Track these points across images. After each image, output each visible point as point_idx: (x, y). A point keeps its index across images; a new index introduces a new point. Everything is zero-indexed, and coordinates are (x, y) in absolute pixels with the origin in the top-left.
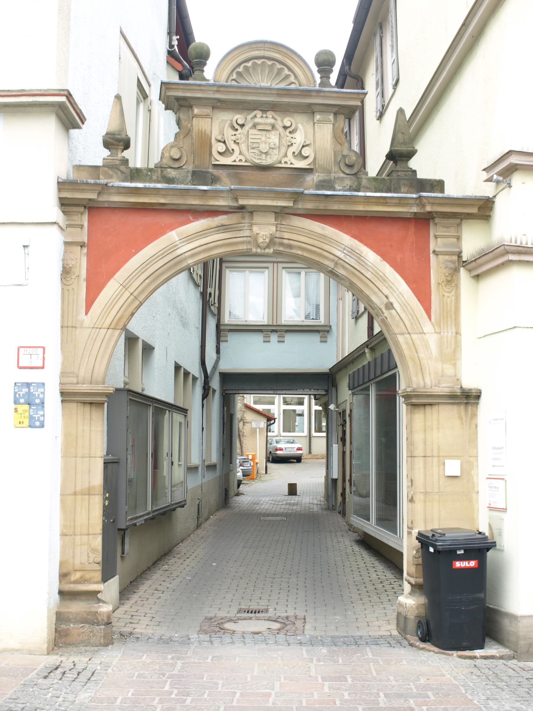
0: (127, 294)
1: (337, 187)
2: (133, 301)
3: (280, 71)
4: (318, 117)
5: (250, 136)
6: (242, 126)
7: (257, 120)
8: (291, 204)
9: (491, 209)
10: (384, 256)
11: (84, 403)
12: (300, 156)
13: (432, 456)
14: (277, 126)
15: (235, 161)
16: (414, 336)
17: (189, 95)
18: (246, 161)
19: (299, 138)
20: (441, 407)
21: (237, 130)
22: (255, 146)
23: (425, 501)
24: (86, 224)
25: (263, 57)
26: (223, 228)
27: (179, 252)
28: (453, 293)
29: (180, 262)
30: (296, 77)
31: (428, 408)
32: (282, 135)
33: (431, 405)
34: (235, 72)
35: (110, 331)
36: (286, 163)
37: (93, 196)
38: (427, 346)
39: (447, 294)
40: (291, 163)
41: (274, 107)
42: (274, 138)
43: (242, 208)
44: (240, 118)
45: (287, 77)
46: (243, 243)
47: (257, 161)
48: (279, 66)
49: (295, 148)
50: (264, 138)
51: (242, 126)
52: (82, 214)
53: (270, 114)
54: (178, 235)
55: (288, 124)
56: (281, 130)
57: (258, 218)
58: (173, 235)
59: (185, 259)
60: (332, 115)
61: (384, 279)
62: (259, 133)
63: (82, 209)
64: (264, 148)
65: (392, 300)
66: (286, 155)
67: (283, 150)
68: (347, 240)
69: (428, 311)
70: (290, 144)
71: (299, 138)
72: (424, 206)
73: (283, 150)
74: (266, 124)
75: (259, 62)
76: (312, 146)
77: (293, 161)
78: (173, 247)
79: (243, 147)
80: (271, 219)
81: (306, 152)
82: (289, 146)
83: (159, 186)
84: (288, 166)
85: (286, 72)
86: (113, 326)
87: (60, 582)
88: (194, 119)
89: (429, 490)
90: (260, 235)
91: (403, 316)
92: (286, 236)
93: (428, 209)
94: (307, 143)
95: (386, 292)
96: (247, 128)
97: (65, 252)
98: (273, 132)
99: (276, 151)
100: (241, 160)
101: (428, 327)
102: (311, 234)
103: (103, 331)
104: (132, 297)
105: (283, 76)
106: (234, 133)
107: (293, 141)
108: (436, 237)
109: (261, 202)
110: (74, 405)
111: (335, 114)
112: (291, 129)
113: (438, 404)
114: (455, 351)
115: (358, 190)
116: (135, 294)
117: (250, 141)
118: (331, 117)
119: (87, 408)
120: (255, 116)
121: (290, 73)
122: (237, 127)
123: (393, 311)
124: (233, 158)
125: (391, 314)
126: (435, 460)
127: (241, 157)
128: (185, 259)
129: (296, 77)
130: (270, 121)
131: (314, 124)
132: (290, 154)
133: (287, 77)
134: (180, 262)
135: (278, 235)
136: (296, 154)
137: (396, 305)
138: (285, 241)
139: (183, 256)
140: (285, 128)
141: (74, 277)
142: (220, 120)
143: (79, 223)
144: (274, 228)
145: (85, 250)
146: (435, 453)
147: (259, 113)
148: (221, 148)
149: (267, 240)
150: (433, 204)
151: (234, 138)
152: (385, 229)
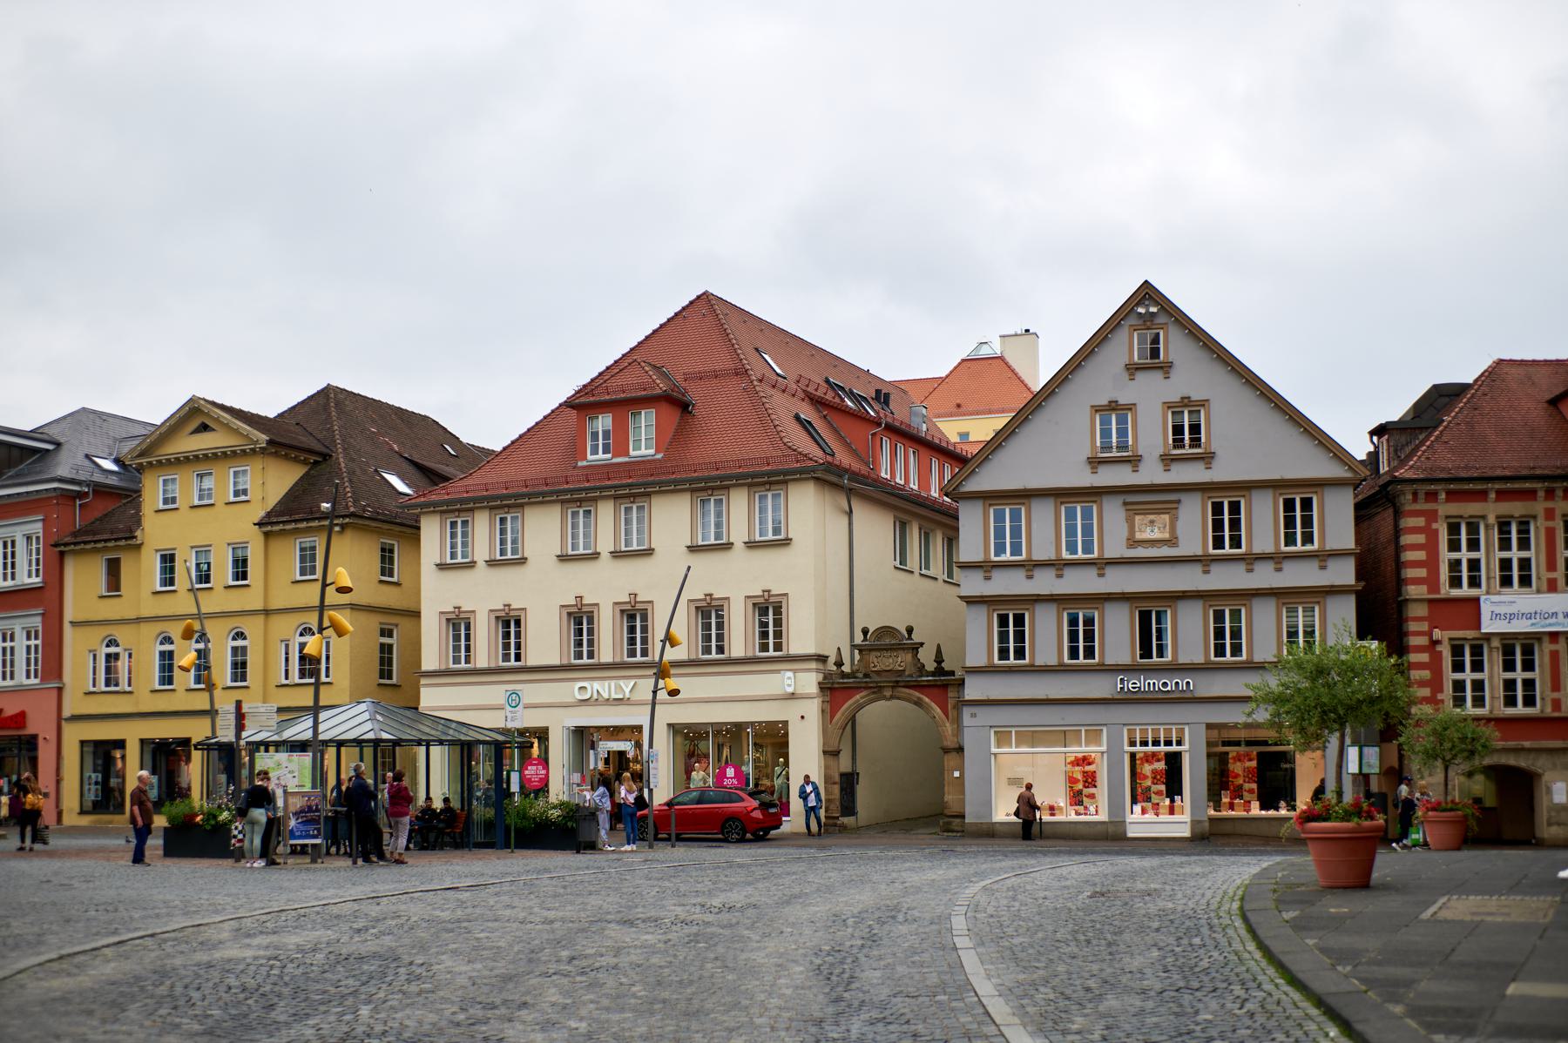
26: (874, 693)
42: (891, 660)
58: (858, 697)
68: (917, 694)
71: (899, 659)
101: (948, 725)
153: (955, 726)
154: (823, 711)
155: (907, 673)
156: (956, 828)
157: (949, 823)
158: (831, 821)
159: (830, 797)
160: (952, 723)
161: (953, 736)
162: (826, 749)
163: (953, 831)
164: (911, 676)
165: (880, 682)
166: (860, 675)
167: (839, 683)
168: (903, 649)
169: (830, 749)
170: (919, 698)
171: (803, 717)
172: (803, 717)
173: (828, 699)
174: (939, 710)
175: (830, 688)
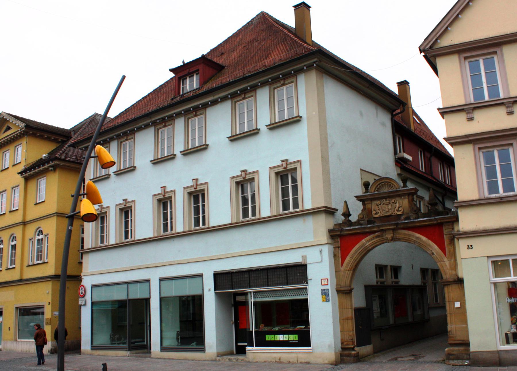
0: (353, 260)
1: (411, 218)
4: (402, 197)
5: (383, 207)
6: (380, 204)
12: (398, 211)
13: (451, 301)
14: (391, 203)
15: (379, 215)
16: (442, 263)
18: (383, 215)
21: (379, 206)
22: (384, 210)
24: (339, 241)
26: (378, 236)
27: (366, 245)
28: (452, 247)
29: (367, 248)
30: (395, 186)
32: (392, 205)
33: (449, 285)
35: (349, 271)
36: (395, 213)
37: (339, 233)
38: (446, 265)
39: (450, 248)
40: (396, 213)
42: (390, 207)
43: (382, 230)
44: (379, 202)
46: (385, 240)
47: (385, 215)
49: (397, 208)
50: (387, 207)
51: (380, 204)
52: (338, 238)
53: (388, 199)
54: (365, 240)
55: (393, 201)
56: (392, 203)
57: (387, 232)
58: (364, 241)
59: (368, 247)
60: (407, 196)
61: (430, 245)
63: (337, 237)
65: (433, 252)
66: (394, 211)
67: (393, 210)
71: (397, 205)
73: (393, 210)
74: (387, 203)
75: (383, 184)
76: (402, 207)
77: (397, 212)
78: (364, 244)
79: (381, 211)
81: (400, 209)
84: (395, 214)
85: (392, 185)
86: (350, 270)
89: (451, 312)
90: (388, 237)
91: (437, 256)
94: (401, 206)
95: (431, 249)
96: (382, 205)
98: (389, 205)
99: (391, 210)
100: (381, 215)
101: (445, 259)
103: (347, 271)
104: (354, 261)
105: (391, 186)
106: (378, 207)
107: (396, 206)
112: (395, 203)
113: (451, 284)
115: (418, 218)
116: (355, 259)
117: (383, 208)
118: (407, 197)
120: (384, 201)
121: (393, 185)
122: (379, 205)
123: (434, 255)
124: (379, 214)
125: (433, 256)
126: (452, 302)
127: (381, 214)
128: (368, 247)
129: (395, 186)
130: (388, 201)
132: (395, 210)
133: (393, 186)
134: (367, 248)
135: (395, 236)
137: (435, 253)
138: (398, 238)
139: (367, 247)
140: (393, 203)
141: (337, 257)
142: (374, 204)
143: (337, 241)
145: (340, 248)
146: (452, 301)
147: (384, 200)
149: (391, 238)
151: (378, 208)
154: (335, 256)
168: (400, 196)
174: (436, 247)
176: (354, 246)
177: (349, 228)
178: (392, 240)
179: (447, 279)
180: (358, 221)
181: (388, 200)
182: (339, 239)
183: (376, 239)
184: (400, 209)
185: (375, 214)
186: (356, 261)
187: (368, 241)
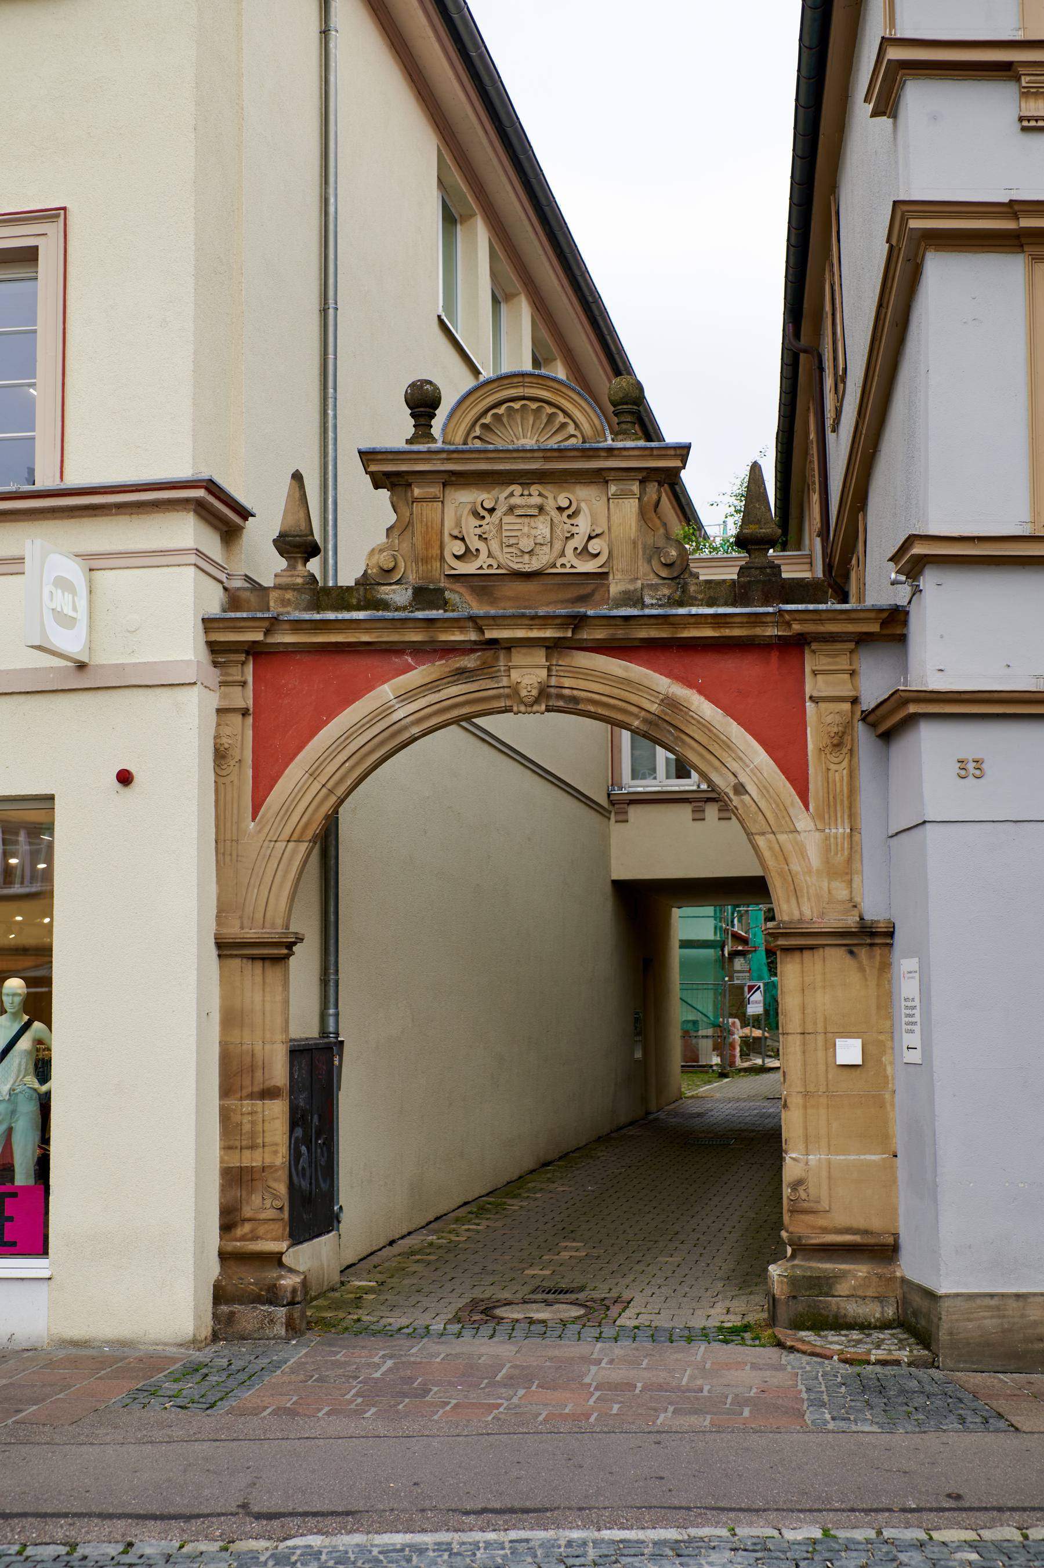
0: (317, 786)
1: (648, 600)
2: (326, 798)
3: (551, 417)
4: (613, 489)
5: (505, 527)
6: (492, 511)
7: (514, 501)
8: (569, 634)
9: (905, 623)
10: (729, 712)
11: (253, 958)
12: (584, 552)
13: (815, 1033)
14: (548, 508)
15: (481, 568)
16: (782, 837)
17: (404, 468)
18: (499, 567)
19: (583, 525)
20: (828, 950)
21: (483, 518)
22: (512, 541)
23: (805, 1107)
24: (250, 680)
25: (524, 398)
26: (461, 674)
27: (396, 716)
28: (845, 764)
29: (399, 732)
30: (577, 426)
31: (807, 954)
32: (555, 521)
33: (812, 948)
34: (478, 424)
35: (291, 844)
36: (563, 565)
37: (259, 637)
38: (802, 852)
39: (833, 767)
40: (572, 567)
41: (541, 477)
42: (542, 528)
43: (494, 642)
44: (484, 497)
45: (564, 426)
46: (498, 697)
47: (516, 567)
48: (550, 410)
49: (578, 542)
50: (526, 529)
51: (492, 511)
52: (243, 663)
53: (534, 489)
54: (393, 690)
55: (565, 503)
56: (554, 513)
57: (518, 658)
58: (386, 692)
59: (406, 728)
60: (638, 483)
61: (727, 745)
62: (519, 520)
63: (242, 657)
64: (526, 544)
65: (743, 778)
66: (562, 554)
67: (558, 546)
68: (663, 684)
69: (804, 795)
70: (569, 535)
71: (583, 525)
72: (788, 624)
73: (558, 546)
74: (529, 507)
75: (517, 405)
76: (606, 536)
77: (575, 562)
78: (386, 711)
79: (494, 545)
80: (539, 657)
81: (594, 546)
82: (567, 538)
83: (361, 615)
84: (567, 570)
85: (561, 418)
86: (295, 837)
87: (221, 1239)
88: (415, 504)
89: (811, 1088)
90: (523, 685)
91: (763, 804)
92: (567, 682)
93: (796, 627)
94: (598, 531)
95: (734, 766)
96: (498, 513)
97: (218, 725)
98: (541, 518)
99: (546, 549)
100: (490, 566)
101: (803, 821)
102: (605, 677)
103: (281, 845)
104: (324, 790)
105: (557, 425)
106: (478, 523)
107: (575, 530)
108: (815, 673)
109: (520, 633)
110: (237, 962)
111: (642, 482)
112: (570, 512)
113: (824, 946)
114: (850, 860)
115: (681, 604)
116: (329, 785)
117: (505, 534)
118: (635, 487)
119: (259, 964)
120: (512, 494)
121: (567, 420)
122: (483, 513)
123: (746, 798)
124: (478, 563)
125: (743, 802)
126: (820, 1038)
127: (490, 561)
128: (406, 728)
129: (577, 426)
130: (536, 500)
131: (608, 500)
132: (569, 551)
133: (564, 426)
134: (399, 732)
135: (553, 681)
136: (578, 551)
137: (751, 788)
138: (566, 692)
139: (403, 722)
140: (560, 509)
141: (232, 763)
142: (457, 504)
143: (239, 678)
144: (544, 673)
145: (250, 720)
146: (820, 1028)
147: (517, 489)
148: (459, 548)
149: (535, 693)
150: (801, 621)
151: (478, 531)
152: (729, 665)
153: (842, 830)
154: (220, 755)
155: (616, 587)
156: (853, 1309)
157: (822, 1285)
158: (250, 1278)
159: (251, 1159)
160: (824, 818)
161: (831, 872)
162: (234, 931)
163: (840, 1324)
164: (633, 599)
165: (496, 621)
166: (400, 595)
167: (297, 625)
168: (599, 478)
169: (251, 934)
170: (671, 703)
171: (125, 778)
172: (125, 778)
173: (244, 698)
174: (760, 757)
175: (255, 652)
176: (331, 717)
177: (307, 616)
178: (537, 701)
179: (800, 921)
180: (365, 582)
181: (535, 493)
182: (250, 668)
183: (454, 690)
184: (594, 546)
185: (457, 557)
186: (331, 791)
187: (406, 696)
